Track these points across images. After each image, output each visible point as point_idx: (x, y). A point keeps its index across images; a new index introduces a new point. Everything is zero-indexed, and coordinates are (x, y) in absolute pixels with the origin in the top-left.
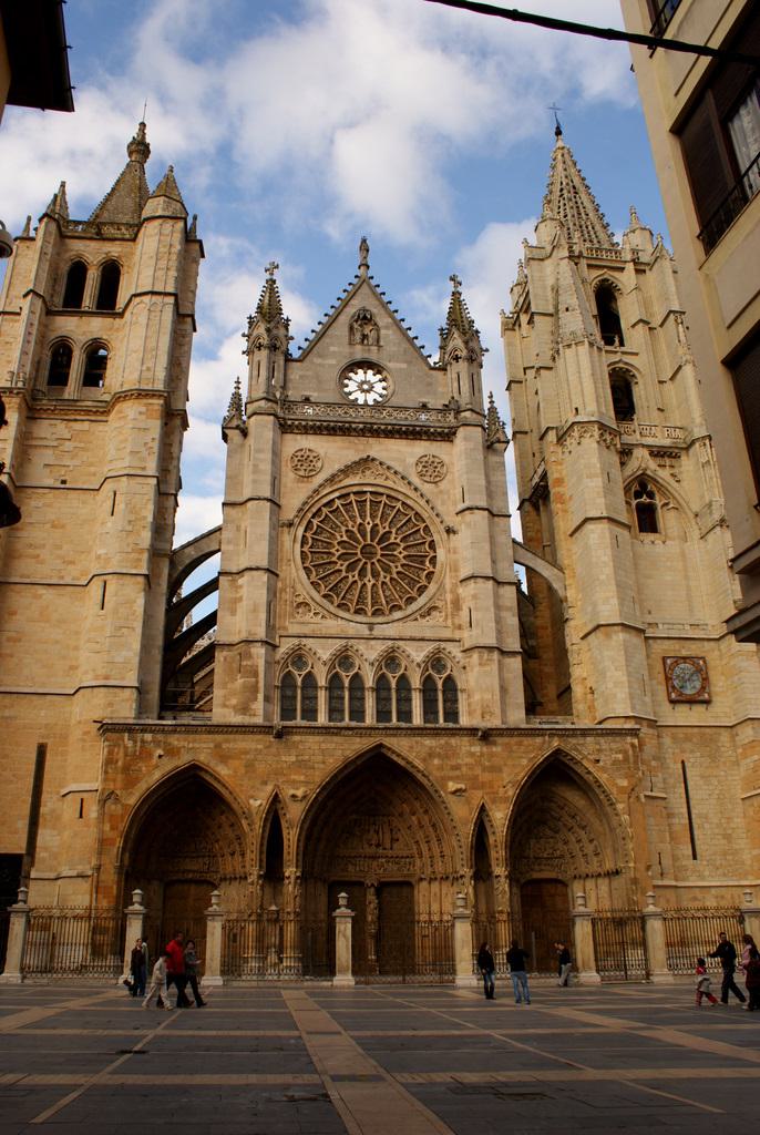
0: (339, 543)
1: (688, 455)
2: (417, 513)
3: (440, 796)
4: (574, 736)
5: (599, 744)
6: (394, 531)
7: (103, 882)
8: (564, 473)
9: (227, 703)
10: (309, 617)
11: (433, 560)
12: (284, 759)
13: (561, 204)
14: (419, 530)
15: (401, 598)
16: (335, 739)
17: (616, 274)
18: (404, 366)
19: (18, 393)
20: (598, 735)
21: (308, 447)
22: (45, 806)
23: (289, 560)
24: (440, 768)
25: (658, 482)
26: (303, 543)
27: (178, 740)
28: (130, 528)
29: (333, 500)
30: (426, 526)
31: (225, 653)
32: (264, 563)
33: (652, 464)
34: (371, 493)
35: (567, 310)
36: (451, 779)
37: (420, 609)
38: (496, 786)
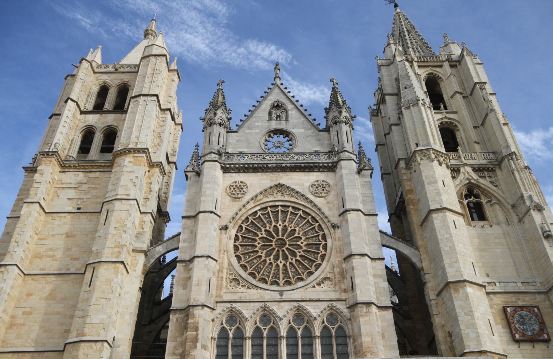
0: (259, 239)
1: (500, 168)
2: (313, 217)
6: (297, 229)
8: (412, 186)
11: (325, 247)
13: (400, 40)
14: (314, 227)
15: (303, 273)
17: (438, 69)
18: (303, 130)
19: (52, 155)
21: (240, 180)
23: (225, 251)
25: (480, 187)
28: (115, 232)
29: (256, 212)
30: (320, 225)
31: (177, 316)
32: (206, 253)
33: (474, 176)
34: (282, 206)
35: (406, 88)
37: (316, 279)
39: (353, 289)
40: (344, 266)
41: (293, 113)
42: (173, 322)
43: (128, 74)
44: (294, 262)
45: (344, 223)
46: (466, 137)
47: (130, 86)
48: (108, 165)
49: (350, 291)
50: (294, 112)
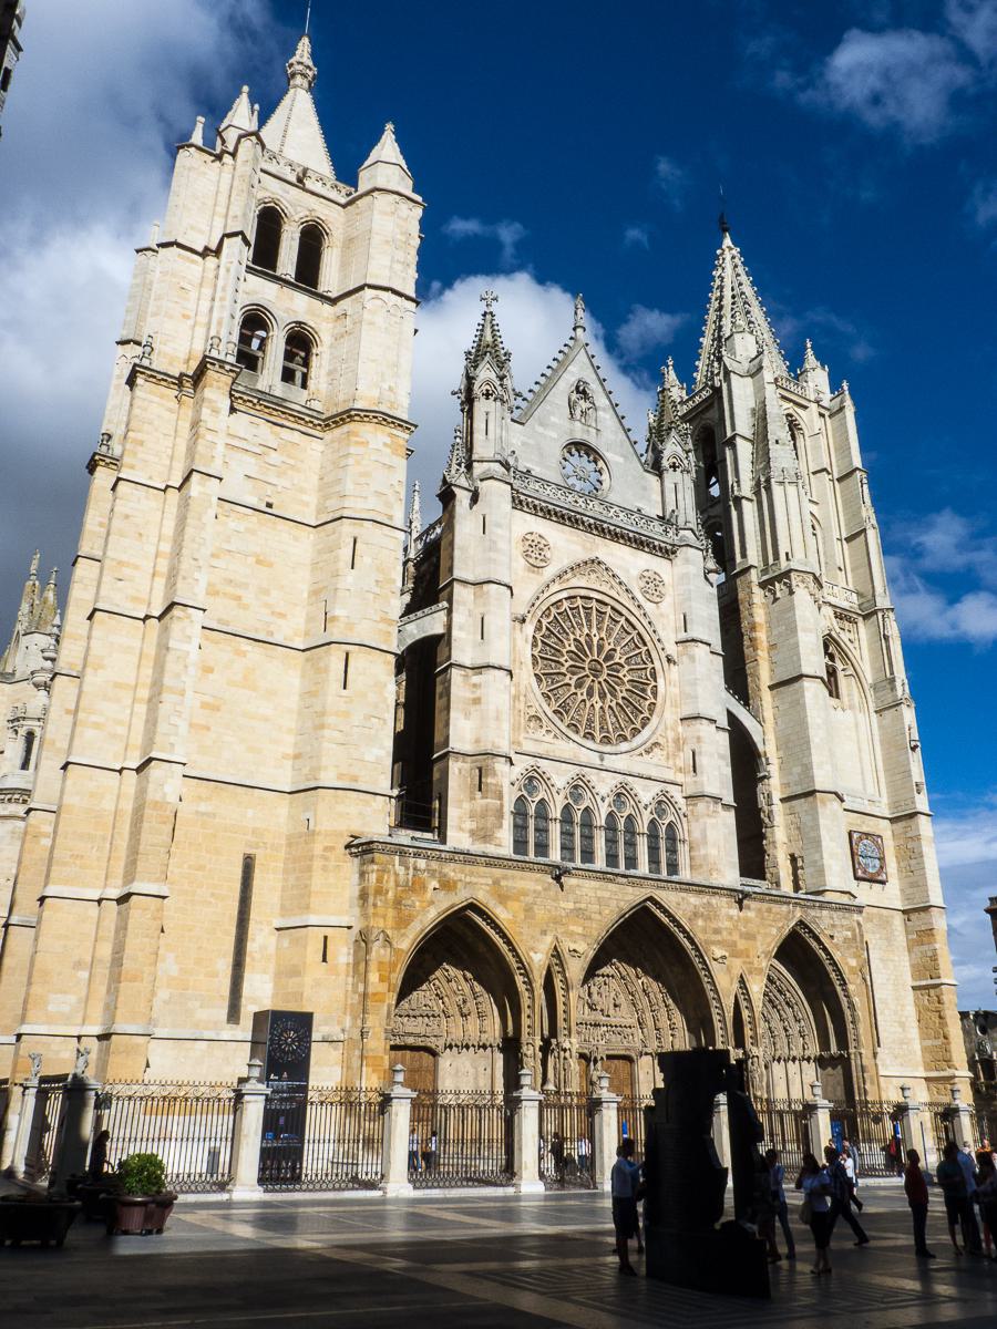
2: (639, 634)
3: (704, 963)
4: (821, 908)
5: (833, 918)
6: (618, 649)
7: (372, 1050)
9: (463, 826)
10: (540, 734)
12: (563, 905)
16: (610, 885)
17: (799, 411)
18: (621, 460)
19: (231, 371)
20: (832, 909)
22: (253, 940)
24: (704, 931)
26: (534, 645)
27: (454, 871)
28: (377, 590)
29: (560, 601)
30: (648, 650)
31: (460, 764)
34: (597, 601)
35: (777, 442)
36: (718, 943)
38: (751, 955)
39: (695, 771)
40: (680, 729)
41: (606, 418)
42: (454, 773)
43: (322, 200)
44: (613, 704)
45: (685, 658)
46: (825, 553)
47: (327, 234)
48: (316, 422)
49: (689, 772)
50: (608, 416)
